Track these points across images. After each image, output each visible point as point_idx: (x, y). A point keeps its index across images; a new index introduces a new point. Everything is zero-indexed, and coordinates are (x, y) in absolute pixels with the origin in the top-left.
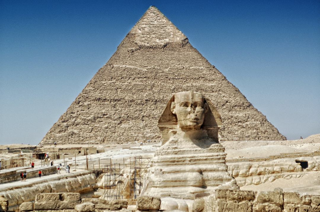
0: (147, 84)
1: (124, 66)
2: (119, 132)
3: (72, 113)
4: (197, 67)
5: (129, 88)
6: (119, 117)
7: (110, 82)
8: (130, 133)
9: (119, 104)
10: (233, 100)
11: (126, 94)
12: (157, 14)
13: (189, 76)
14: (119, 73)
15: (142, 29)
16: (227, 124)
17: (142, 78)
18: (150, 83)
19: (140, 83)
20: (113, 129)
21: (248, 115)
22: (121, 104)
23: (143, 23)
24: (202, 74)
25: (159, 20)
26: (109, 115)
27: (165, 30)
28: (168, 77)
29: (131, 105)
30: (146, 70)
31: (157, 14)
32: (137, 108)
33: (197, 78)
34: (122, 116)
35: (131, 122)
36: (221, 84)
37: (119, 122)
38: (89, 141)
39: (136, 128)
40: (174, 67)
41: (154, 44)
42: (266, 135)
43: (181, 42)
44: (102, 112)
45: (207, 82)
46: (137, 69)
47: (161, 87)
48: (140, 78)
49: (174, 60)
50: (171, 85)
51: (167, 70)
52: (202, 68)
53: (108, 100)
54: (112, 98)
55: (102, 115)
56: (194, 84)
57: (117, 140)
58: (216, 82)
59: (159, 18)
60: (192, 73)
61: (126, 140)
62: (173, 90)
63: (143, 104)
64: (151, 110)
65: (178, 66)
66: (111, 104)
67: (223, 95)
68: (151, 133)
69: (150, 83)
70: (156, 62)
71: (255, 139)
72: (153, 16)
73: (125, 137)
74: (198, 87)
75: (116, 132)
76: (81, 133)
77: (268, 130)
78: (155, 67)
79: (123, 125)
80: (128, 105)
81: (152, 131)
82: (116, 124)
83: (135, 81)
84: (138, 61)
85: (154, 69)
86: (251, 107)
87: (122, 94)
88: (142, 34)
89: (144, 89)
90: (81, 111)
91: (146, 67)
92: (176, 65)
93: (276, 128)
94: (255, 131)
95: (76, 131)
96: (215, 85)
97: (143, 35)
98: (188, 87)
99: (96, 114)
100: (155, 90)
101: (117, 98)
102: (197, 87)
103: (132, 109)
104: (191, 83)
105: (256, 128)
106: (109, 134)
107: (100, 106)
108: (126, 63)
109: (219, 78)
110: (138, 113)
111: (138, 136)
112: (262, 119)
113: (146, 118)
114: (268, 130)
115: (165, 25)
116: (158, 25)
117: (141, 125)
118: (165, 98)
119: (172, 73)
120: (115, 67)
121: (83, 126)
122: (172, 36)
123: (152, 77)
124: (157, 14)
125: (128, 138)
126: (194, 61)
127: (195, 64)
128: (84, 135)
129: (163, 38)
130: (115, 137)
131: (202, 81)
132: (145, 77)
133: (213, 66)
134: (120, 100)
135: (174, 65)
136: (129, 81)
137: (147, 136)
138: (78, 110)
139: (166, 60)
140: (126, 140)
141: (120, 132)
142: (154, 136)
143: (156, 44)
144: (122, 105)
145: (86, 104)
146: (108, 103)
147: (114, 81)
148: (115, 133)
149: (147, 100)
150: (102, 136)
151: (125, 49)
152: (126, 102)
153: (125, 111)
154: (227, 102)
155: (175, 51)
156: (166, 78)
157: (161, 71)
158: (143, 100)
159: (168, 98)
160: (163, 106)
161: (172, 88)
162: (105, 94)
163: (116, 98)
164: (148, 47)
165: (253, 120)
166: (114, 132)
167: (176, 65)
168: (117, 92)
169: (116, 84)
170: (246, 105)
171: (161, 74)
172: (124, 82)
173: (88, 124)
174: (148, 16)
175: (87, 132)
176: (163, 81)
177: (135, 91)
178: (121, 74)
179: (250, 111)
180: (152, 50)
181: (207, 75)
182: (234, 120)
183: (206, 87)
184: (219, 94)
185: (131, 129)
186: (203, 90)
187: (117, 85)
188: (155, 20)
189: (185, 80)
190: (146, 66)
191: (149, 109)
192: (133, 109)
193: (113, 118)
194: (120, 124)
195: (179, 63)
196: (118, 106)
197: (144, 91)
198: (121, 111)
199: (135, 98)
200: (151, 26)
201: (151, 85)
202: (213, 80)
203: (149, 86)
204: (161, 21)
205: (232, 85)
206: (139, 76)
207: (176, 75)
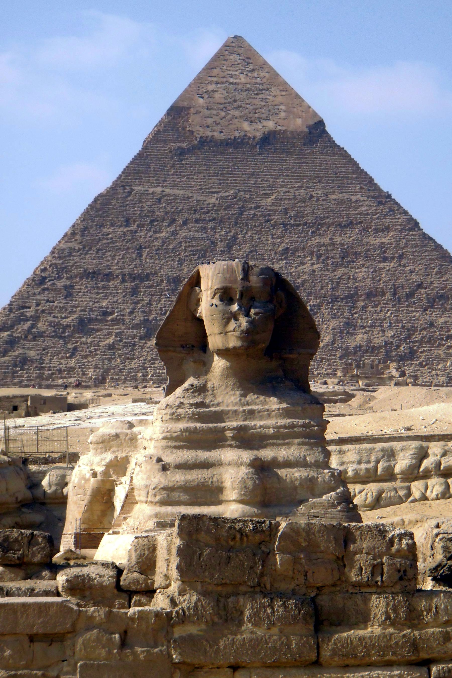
0: (217, 236)
1: (159, 189)
3: (24, 307)
4: (346, 196)
5: (171, 247)
11: (161, 263)
12: (247, 58)
14: (147, 207)
15: (207, 96)
16: (417, 341)
17: (204, 220)
19: (197, 235)
23: (210, 79)
24: (358, 214)
25: (250, 72)
27: (266, 99)
30: (213, 200)
31: (247, 58)
34: (150, 318)
37: (142, 332)
38: (65, 380)
41: (237, 134)
43: (307, 130)
44: (101, 307)
45: (372, 234)
46: (191, 197)
47: (253, 246)
49: (288, 176)
50: (279, 240)
51: (269, 201)
54: (126, 271)
55: (101, 314)
57: (136, 379)
59: (251, 67)
60: (331, 210)
62: (283, 254)
67: (408, 268)
70: (240, 180)
72: (236, 63)
73: (158, 371)
76: (47, 359)
78: (239, 195)
84: (195, 177)
88: (207, 109)
89: (209, 249)
90: (48, 304)
95: (32, 354)
96: (389, 241)
97: (210, 109)
99: (85, 311)
107: (96, 291)
109: (401, 225)
115: (265, 87)
116: (248, 86)
119: (281, 208)
121: (49, 342)
122: (283, 114)
124: (247, 56)
128: (52, 365)
129: (260, 120)
133: (388, 192)
135: (287, 190)
138: (40, 300)
139: (266, 175)
143: (242, 134)
145: (60, 284)
150: (100, 366)
151: (162, 147)
152: (162, 281)
154: (420, 286)
155: (291, 153)
157: (253, 205)
161: (280, 249)
162: (109, 261)
163: (135, 272)
164: (222, 142)
166: (128, 358)
167: (292, 190)
168: (140, 255)
169: (137, 234)
171: (252, 212)
173: (65, 337)
174: (225, 62)
175: (62, 358)
176: (258, 231)
180: (231, 150)
181: (369, 217)
182: (438, 333)
187: (141, 236)
188: (240, 71)
200: (231, 87)
204: (255, 74)
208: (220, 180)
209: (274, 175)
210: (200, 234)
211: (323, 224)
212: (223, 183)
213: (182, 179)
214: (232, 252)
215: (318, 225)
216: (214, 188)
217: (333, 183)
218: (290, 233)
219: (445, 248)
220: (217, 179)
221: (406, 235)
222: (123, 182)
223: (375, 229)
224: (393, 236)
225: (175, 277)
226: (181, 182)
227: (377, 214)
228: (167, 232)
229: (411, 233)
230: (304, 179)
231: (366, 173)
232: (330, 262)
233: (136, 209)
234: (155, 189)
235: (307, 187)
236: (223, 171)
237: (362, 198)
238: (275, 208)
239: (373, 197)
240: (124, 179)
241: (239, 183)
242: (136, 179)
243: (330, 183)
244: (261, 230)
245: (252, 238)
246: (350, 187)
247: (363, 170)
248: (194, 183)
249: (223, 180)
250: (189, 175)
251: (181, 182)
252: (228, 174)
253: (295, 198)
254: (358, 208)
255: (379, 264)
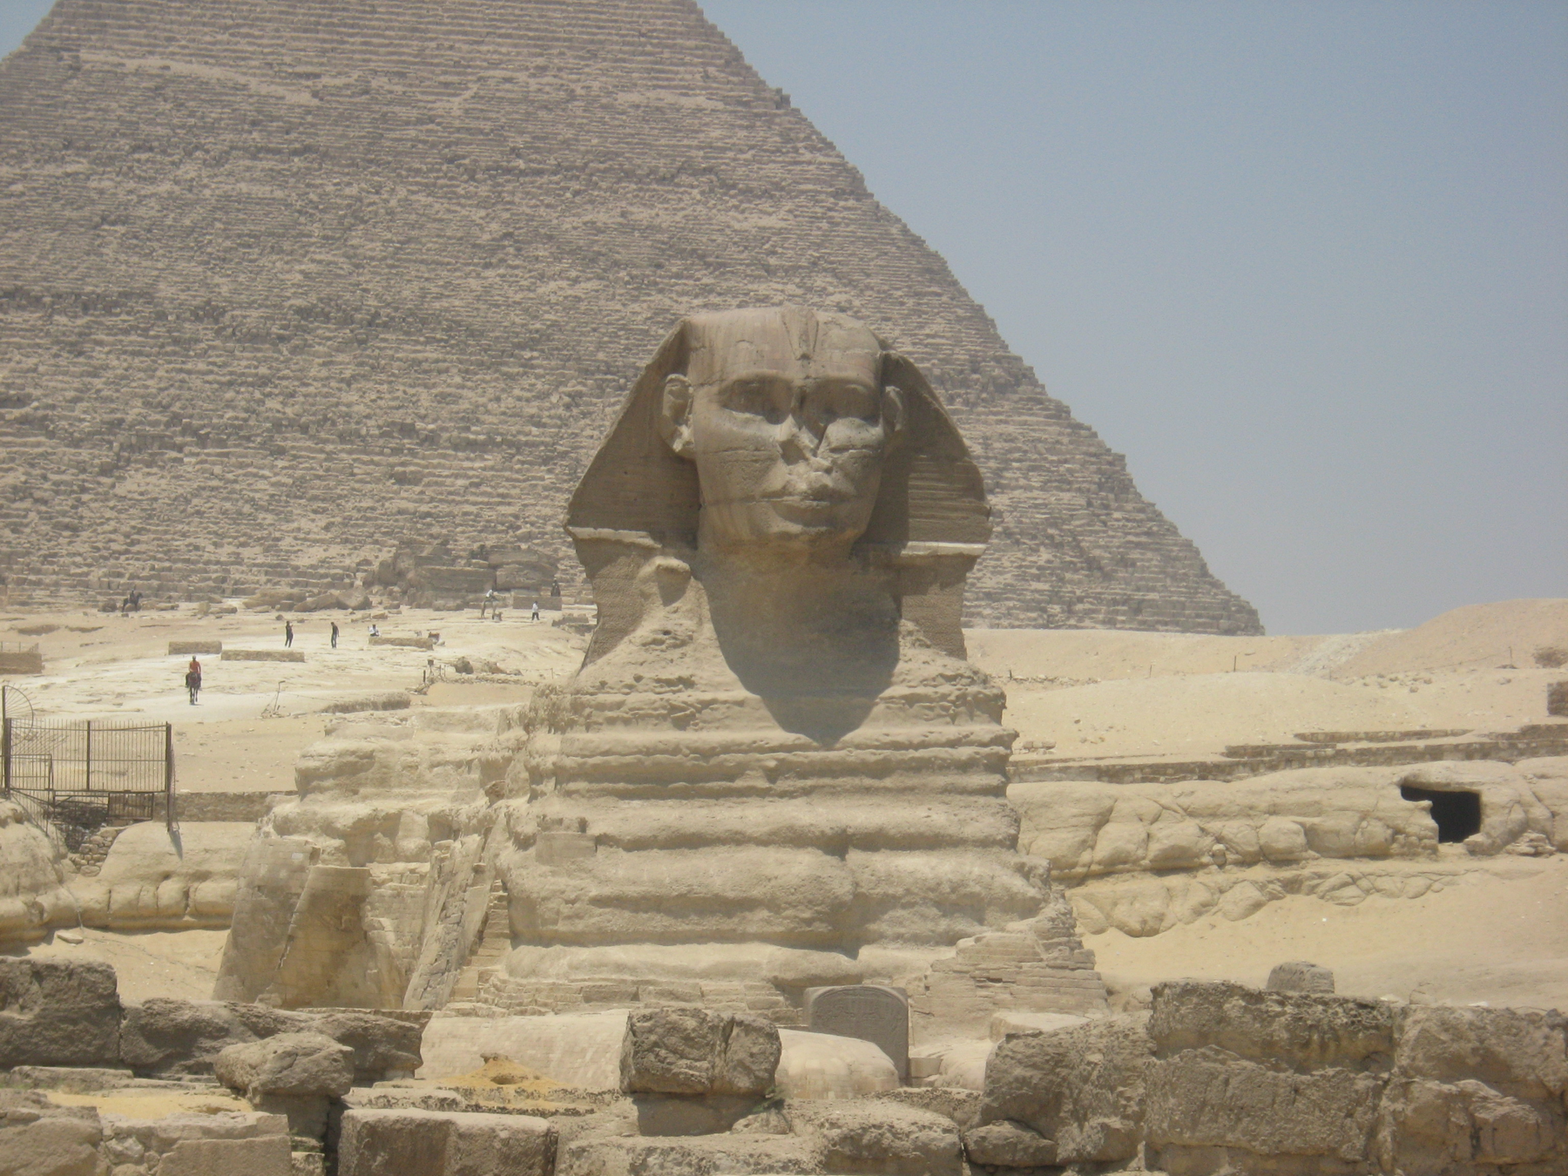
0: (312, 196)
1: (153, 63)
2: (106, 527)
4: (669, 97)
5: (187, 222)
6: (107, 417)
7: (50, 169)
8: (184, 535)
9: (110, 330)
10: (907, 340)
11: (160, 265)
13: (608, 156)
17: (279, 152)
18: (330, 188)
20: (63, 503)
21: (1007, 445)
22: (126, 332)
26: (35, 404)
28: (464, 157)
29: (198, 341)
30: (305, 98)
32: (240, 366)
33: (662, 170)
34: (129, 418)
35: (193, 460)
36: (824, 225)
37: (106, 456)
39: (228, 505)
40: (508, 86)
42: (1117, 589)
45: (735, 202)
46: (245, 87)
48: (269, 151)
49: (509, 36)
50: (483, 213)
51: (456, 105)
52: (701, 100)
53: (38, 300)
54: (61, 286)
56: (641, 214)
57: (87, 585)
58: (789, 205)
61: (155, 583)
62: (493, 252)
63: (281, 338)
64: (333, 384)
65: (532, 81)
66: (53, 329)
68: (331, 542)
69: (330, 188)
71: (1044, 610)
74: (665, 237)
75: (85, 522)
77: (1135, 555)
79: (134, 482)
80: (176, 341)
81: (334, 531)
82: (84, 471)
83: (230, 174)
85: (364, 98)
86: (1024, 388)
87: (135, 259)
91: (308, 76)
92: (522, 77)
93: (1188, 545)
94: (1045, 555)
96: (783, 224)
98: (600, 231)
100: (370, 245)
101: (99, 290)
102: (658, 236)
103: (202, 366)
104: (623, 204)
105: (1052, 537)
106: (34, 538)
108: (170, 39)
109: (817, 181)
110: (241, 397)
111: (238, 561)
112: (1096, 478)
113: (298, 435)
114: (1135, 555)
117: (261, 485)
118: (437, 305)
120: (88, 66)
123: (347, 147)
125: (170, 569)
126: (649, 48)
127: (649, 71)
130: (78, 559)
131: (695, 192)
132: (297, 145)
133: (779, 91)
134: (116, 304)
135: (508, 74)
136: (183, 168)
137: (303, 561)
140: (155, 583)
141: (112, 523)
142: (347, 562)
144: (133, 338)
146: (33, 317)
147: (81, 166)
148: (75, 530)
149: (304, 312)
153: (150, 382)
156: (450, 161)
157: (414, 114)
158: (281, 307)
159: (457, 303)
160: (420, 356)
161: (486, 237)
162: (13, 257)
163: (89, 289)
165: (1036, 480)
166: (67, 527)
167: (522, 77)
169: (93, 184)
170: (997, 372)
171: (413, 133)
172: (151, 173)
176: (426, 185)
177: (228, 243)
178: (128, 117)
179: (1016, 418)
181: (730, 154)
183: (720, 240)
184: (810, 289)
185: (190, 510)
186: (702, 257)
187: (101, 192)
189: (575, 186)
190: (310, 69)
191: (324, 373)
192: (211, 372)
193: (64, 423)
194: (117, 474)
195: (540, 61)
196: (100, 343)
197: (286, 246)
198: (124, 377)
199: (224, 290)
201: (339, 208)
202: (772, 192)
203: (323, 211)
205: (905, 231)
206: (255, 135)
207: (520, 142)
208: (324, 41)
209: (472, 33)
210: (268, 188)
211: (605, 171)
212: (333, 50)
213: (219, 37)
214: (354, 242)
215: (591, 175)
216: (307, 63)
217: (632, 61)
218: (513, 193)
219: (932, 246)
220: (317, 40)
221: (830, 209)
222: (52, 39)
223: (742, 192)
224: (790, 211)
225: (197, 308)
226: (214, 44)
227: (752, 147)
228: (177, 182)
229: (842, 203)
230: (550, 47)
231: (722, 36)
232: (622, 274)
233: (90, 114)
234: (142, 62)
235: (560, 69)
236: (330, 16)
237: (710, 105)
238: (473, 124)
239: (740, 103)
240: (60, 30)
241: (376, 53)
242: (92, 32)
243: (624, 61)
244: (434, 185)
245: (406, 203)
246: (677, 73)
247: (713, 27)
248: (250, 49)
249: (332, 41)
250: (238, 26)
251: (214, 44)
252: (345, 25)
253: (526, 100)
254: (697, 132)
255: (755, 287)
